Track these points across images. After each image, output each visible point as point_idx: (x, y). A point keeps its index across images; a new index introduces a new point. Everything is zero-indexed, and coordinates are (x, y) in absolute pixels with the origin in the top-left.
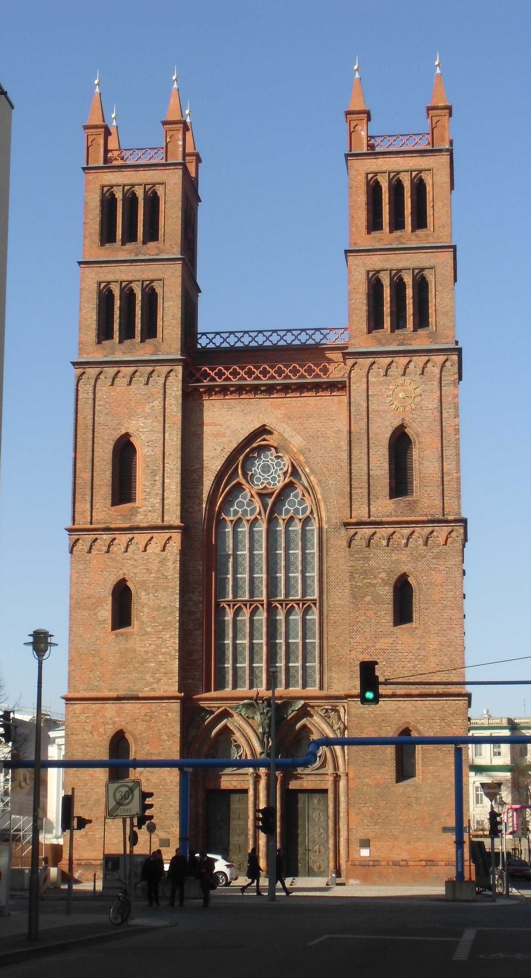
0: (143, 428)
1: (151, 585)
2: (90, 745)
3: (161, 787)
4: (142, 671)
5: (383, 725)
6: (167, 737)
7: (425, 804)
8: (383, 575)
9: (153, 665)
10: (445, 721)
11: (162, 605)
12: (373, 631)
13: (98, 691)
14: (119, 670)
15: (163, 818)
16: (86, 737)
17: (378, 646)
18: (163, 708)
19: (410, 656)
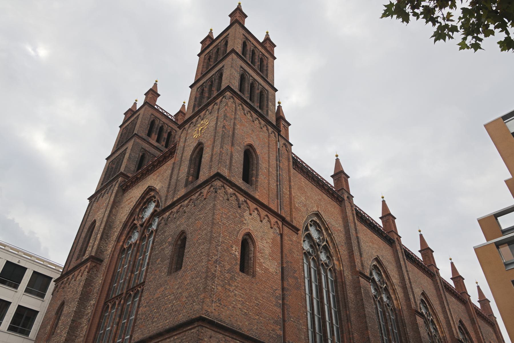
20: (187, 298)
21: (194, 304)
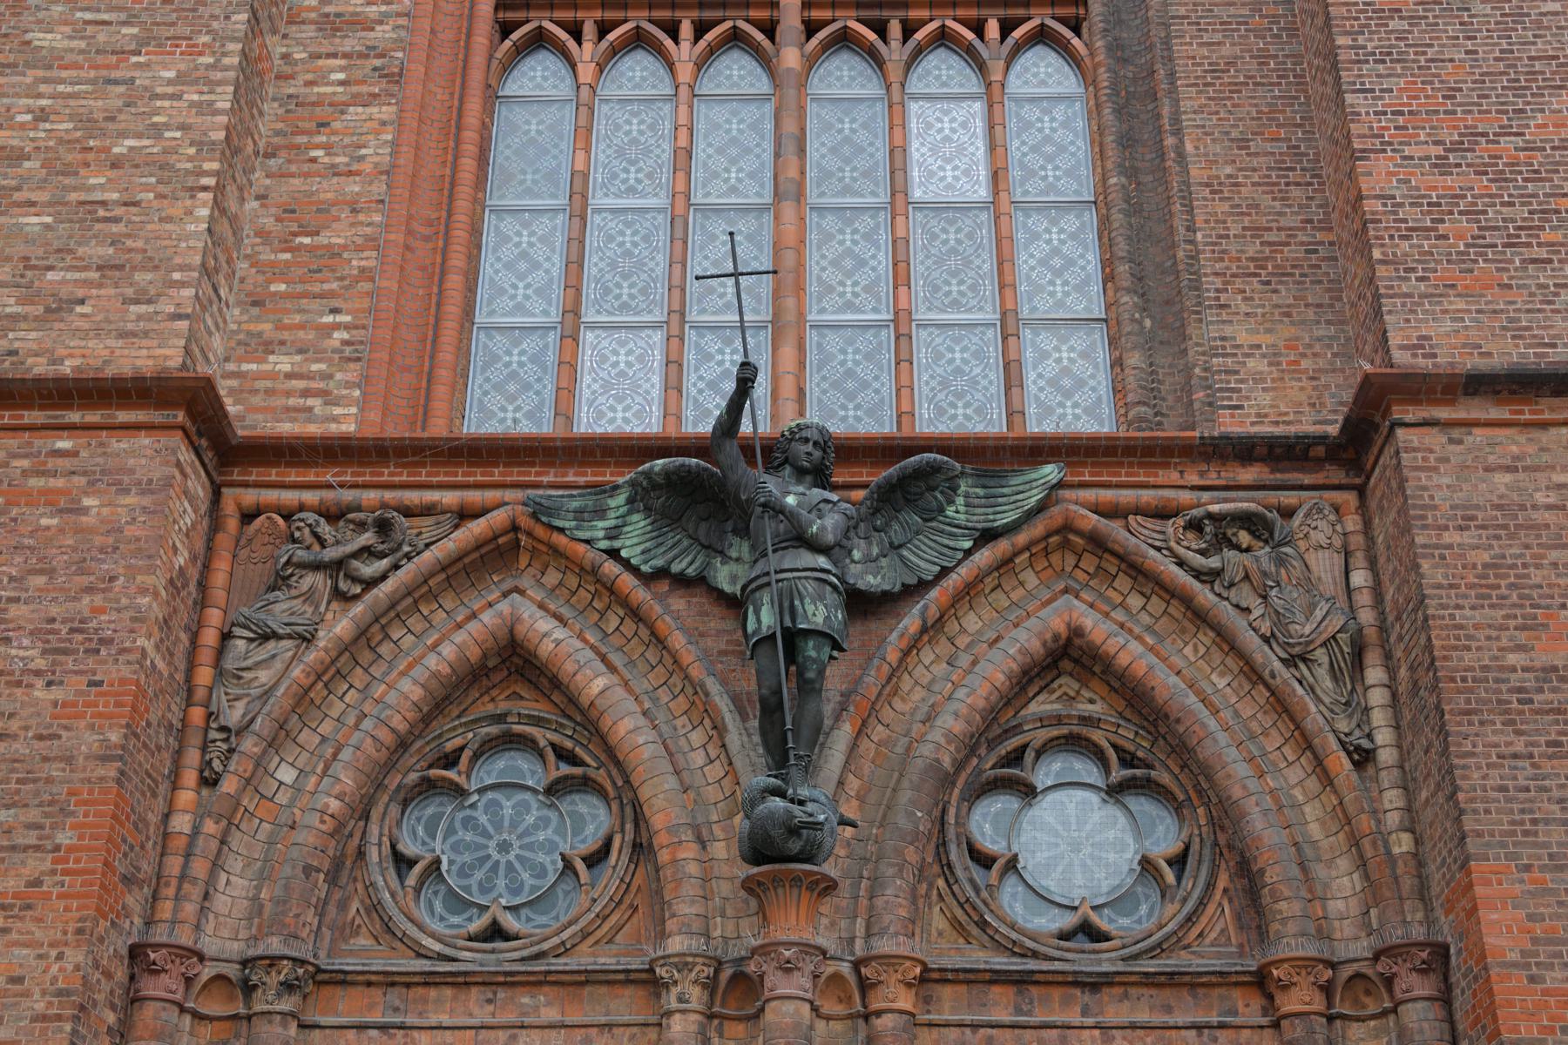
6: (45, 652)
18: (51, 463)
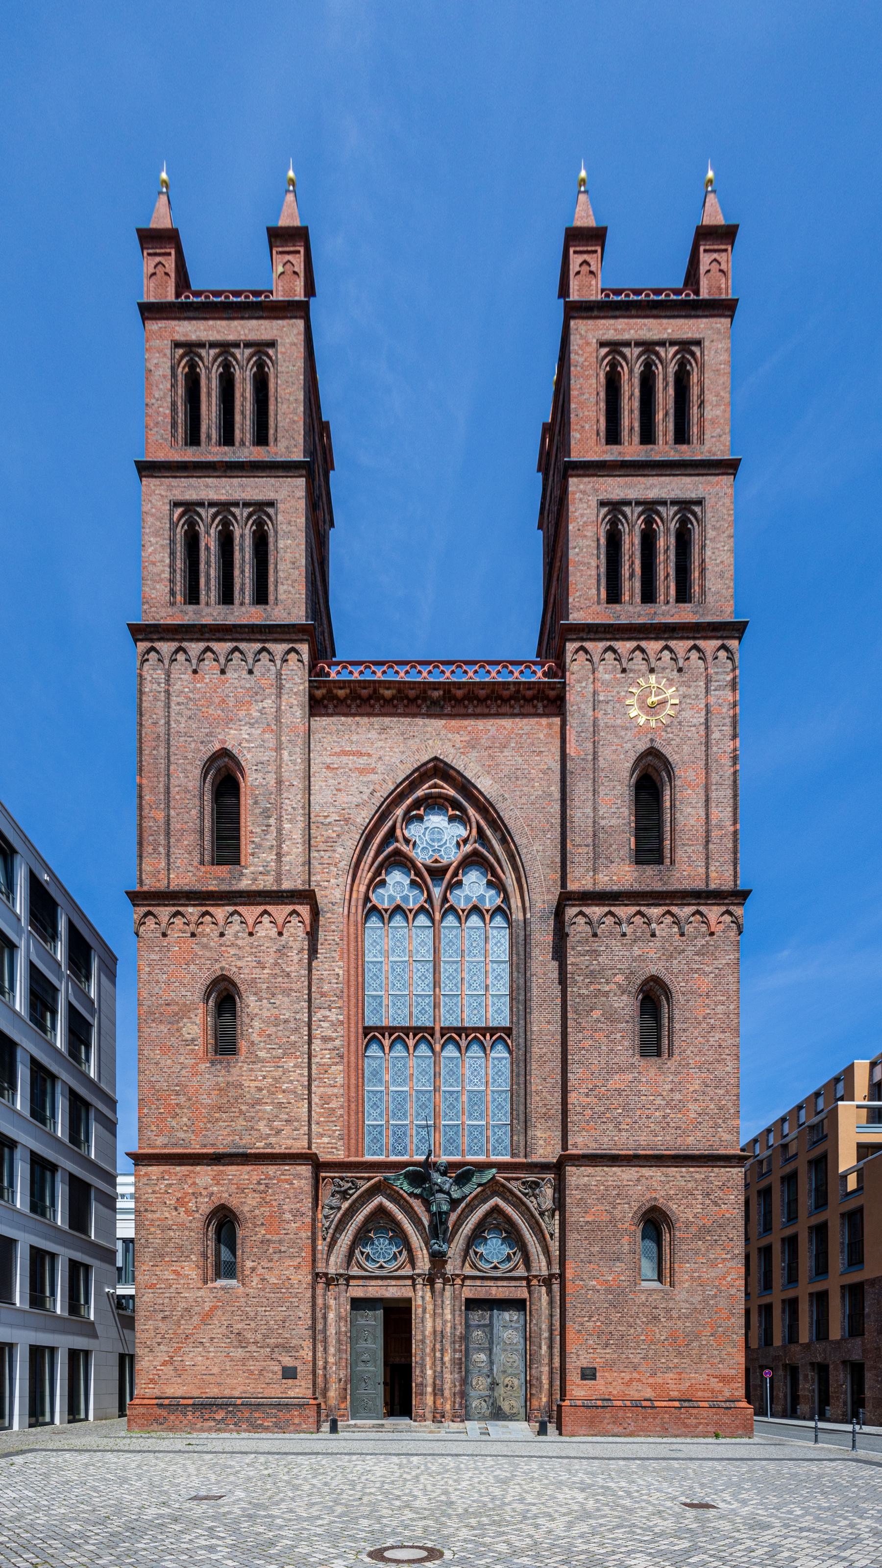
0: (247, 741)
1: (264, 986)
2: (174, 1227)
3: (283, 1290)
4: (253, 1118)
5: (618, 1201)
7: (679, 1318)
8: (620, 978)
9: (268, 1108)
10: (711, 1197)
11: (282, 1017)
12: (603, 1062)
13: (186, 1148)
14: (217, 1115)
15: (289, 1336)
16: (167, 1215)
17: (611, 1085)
19: (659, 1101)
20: (700, 1114)
21: (720, 1129)
